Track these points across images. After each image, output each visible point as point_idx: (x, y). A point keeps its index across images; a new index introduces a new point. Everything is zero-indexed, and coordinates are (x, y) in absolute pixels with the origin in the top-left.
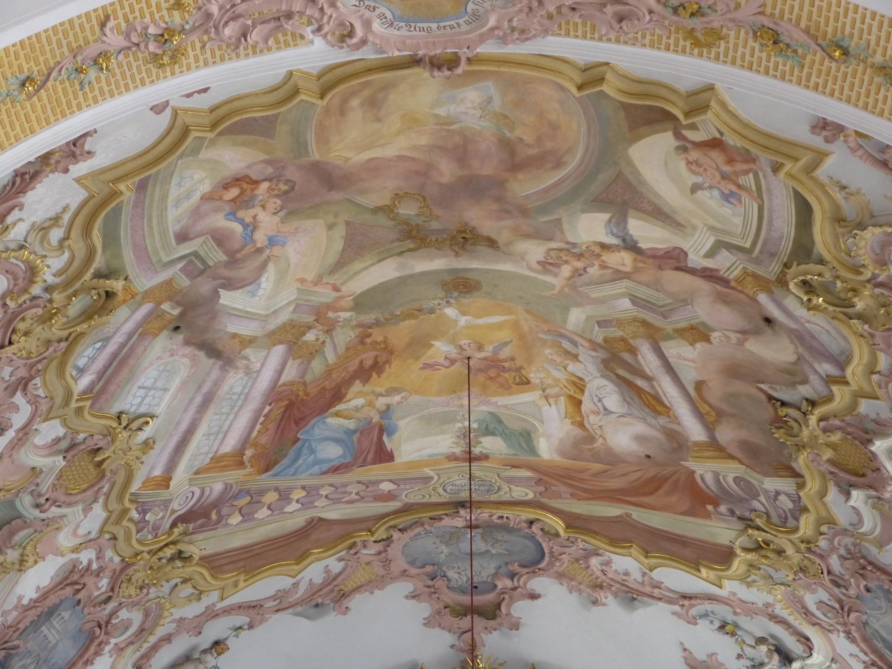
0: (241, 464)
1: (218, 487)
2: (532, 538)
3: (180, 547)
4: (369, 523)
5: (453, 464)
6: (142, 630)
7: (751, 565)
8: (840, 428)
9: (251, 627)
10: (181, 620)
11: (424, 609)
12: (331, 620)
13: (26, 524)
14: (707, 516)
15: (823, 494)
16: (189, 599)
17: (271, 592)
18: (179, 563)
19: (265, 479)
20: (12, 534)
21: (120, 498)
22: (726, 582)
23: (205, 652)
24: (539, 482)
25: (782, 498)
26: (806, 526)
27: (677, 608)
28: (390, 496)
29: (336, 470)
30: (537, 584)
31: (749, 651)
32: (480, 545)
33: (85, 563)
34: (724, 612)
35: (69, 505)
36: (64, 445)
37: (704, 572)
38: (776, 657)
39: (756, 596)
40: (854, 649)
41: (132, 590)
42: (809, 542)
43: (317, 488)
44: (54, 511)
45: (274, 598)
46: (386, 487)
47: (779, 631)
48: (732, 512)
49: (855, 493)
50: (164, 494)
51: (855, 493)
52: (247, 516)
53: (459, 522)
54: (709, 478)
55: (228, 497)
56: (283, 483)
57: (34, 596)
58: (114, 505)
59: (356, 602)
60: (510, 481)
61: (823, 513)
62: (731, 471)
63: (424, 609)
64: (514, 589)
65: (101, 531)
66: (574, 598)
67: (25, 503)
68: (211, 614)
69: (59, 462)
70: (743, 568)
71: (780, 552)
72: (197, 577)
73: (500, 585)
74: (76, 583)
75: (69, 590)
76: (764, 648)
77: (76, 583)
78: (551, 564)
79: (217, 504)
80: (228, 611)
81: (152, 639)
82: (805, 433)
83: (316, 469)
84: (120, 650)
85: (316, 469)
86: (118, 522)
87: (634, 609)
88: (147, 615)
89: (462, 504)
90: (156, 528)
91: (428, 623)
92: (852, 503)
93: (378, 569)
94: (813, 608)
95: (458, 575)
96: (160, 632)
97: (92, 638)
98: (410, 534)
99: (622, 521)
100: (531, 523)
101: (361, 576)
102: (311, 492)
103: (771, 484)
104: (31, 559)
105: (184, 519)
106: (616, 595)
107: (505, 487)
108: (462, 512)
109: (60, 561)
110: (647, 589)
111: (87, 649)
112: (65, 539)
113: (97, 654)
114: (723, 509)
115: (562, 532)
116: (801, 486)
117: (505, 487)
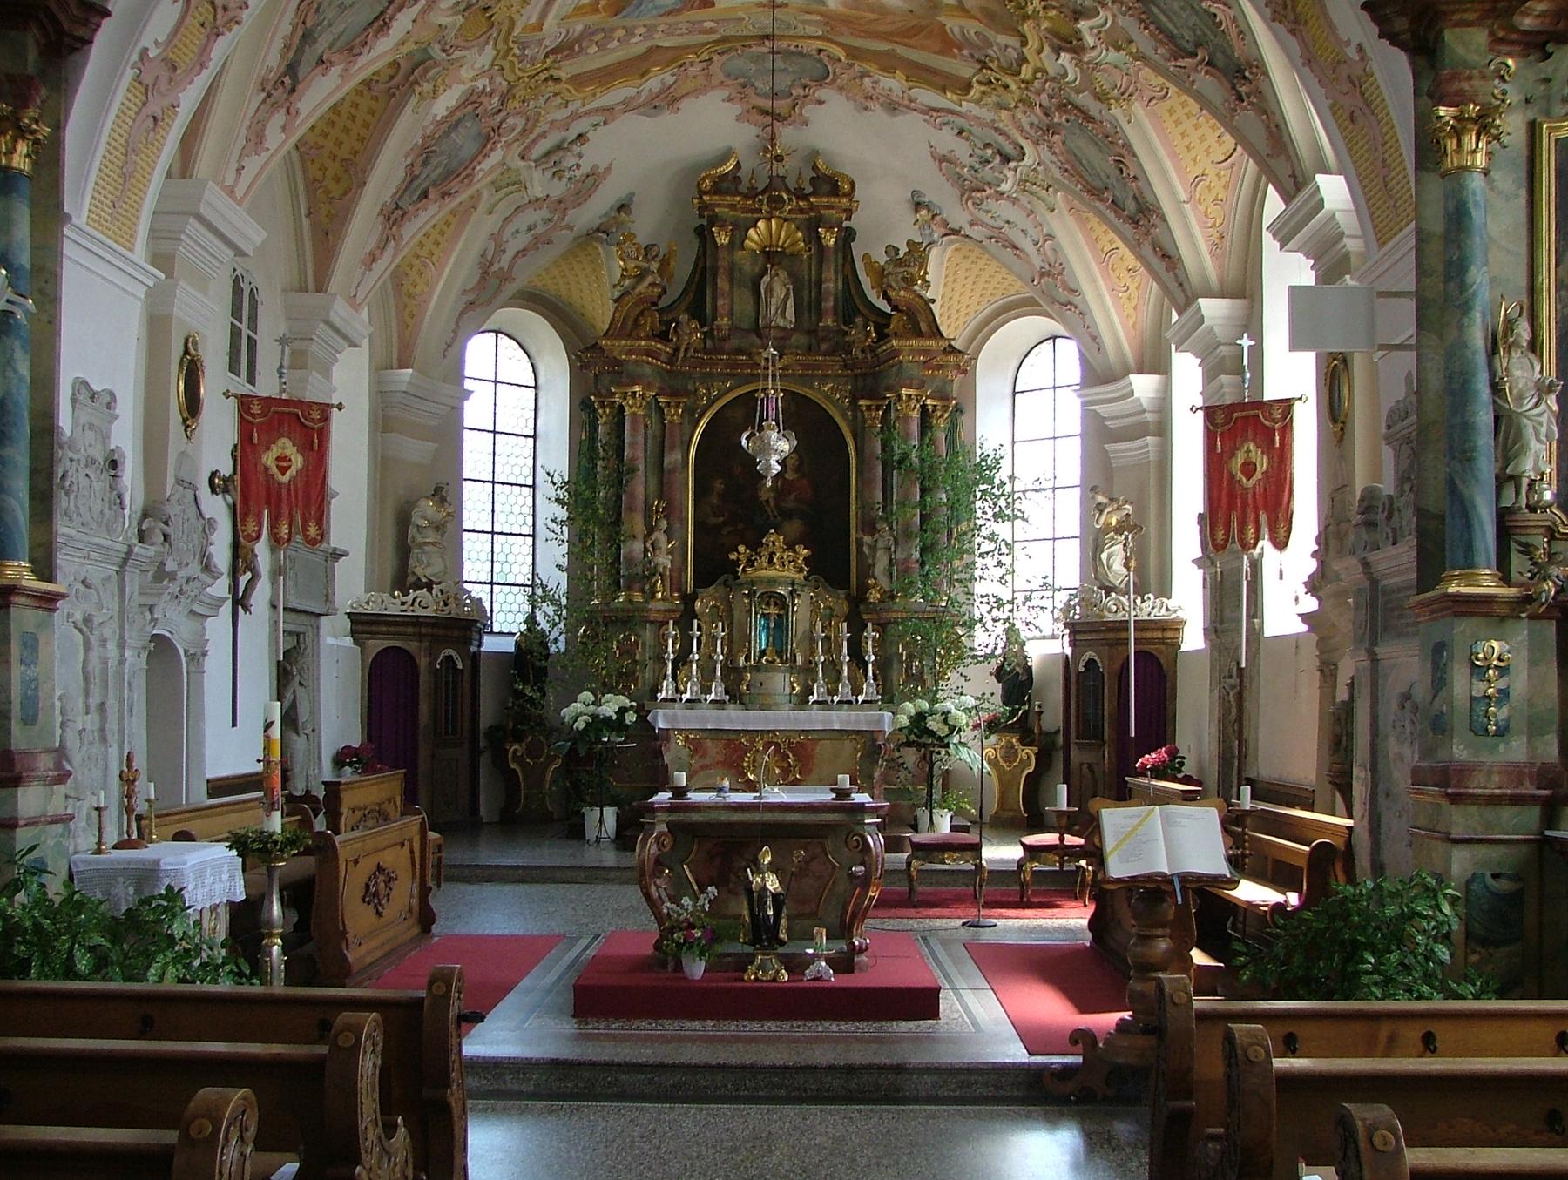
0: (597, 10)
1: (579, 28)
2: (820, 61)
3: (552, 72)
4: (695, 49)
5: (761, 9)
6: (524, 130)
7: (984, 93)
8: (1054, 7)
9: (605, 123)
10: (552, 123)
11: (737, 109)
12: (667, 118)
13: (436, 64)
14: (954, 57)
15: (1040, 51)
16: (559, 106)
17: (620, 99)
18: (550, 83)
19: (616, 21)
20: (426, 71)
21: (506, 41)
22: (964, 103)
23: (572, 142)
24: (826, 24)
25: (1010, 50)
26: (1026, 72)
27: (927, 117)
28: (711, 31)
29: (670, 13)
30: (822, 93)
31: (979, 152)
32: (779, 64)
33: (481, 87)
34: (961, 122)
35: (466, 48)
36: (462, 6)
37: (949, 95)
38: (998, 158)
39: (986, 114)
40: (1054, 158)
41: (517, 104)
42: (1027, 83)
43: (655, 26)
44: (457, 54)
45: (623, 103)
46: (708, 25)
47: (1001, 139)
48: (972, 56)
49: (1063, 54)
50: (539, 35)
51: (1063, 54)
52: (601, 46)
53: (765, 50)
54: (956, 30)
55: (587, 33)
56: (628, 22)
57: (445, 114)
58: (500, 45)
59: (685, 104)
60: (804, 22)
61: (1039, 65)
62: (973, 27)
63: (737, 109)
64: (805, 96)
65: (492, 65)
66: (851, 105)
67: (436, 50)
68: (575, 116)
69: (460, 19)
70: (978, 95)
71: (1006, 87)
72: (565, 91)
73: (794, 93)
74: (475, 102)
75: (470, 108)
76: (989, 152)
77: (475, 102)
78: (834, 81)
79: (578, 40)
80: (586, 114)
81: (532, 137)
82: (1030, 9)
83: (654, 12)
84: (508, 145)
85: (654, 12)
86: (505, 57)
87: (895, 116)
88: (528, 120)
89: (767, 37)
90: (533, 60)
91: (739, 119)
92: (1060, 61)
93: (701, 80)
94: (1027, 127)
95: (763, 85)
96: (537, 131)
97: (488, 138)
98: (726, 57)
99: (887, 53)
100: (820, 51)
101: (689, 85)
102: (651, 29)
103: (1002, 39)
104: (442, 89)
105: (554, 51)
106: (882, 105)
107: (800, 26)
108: (767, 43)
109: (463, 88)
110: (906, 102)
111: (485, 146)
112: (466, 73)
113: (492, 149)
114: (965, 52)
115: (843, 58)
116: (1024, 43)
117: (800, 26)
